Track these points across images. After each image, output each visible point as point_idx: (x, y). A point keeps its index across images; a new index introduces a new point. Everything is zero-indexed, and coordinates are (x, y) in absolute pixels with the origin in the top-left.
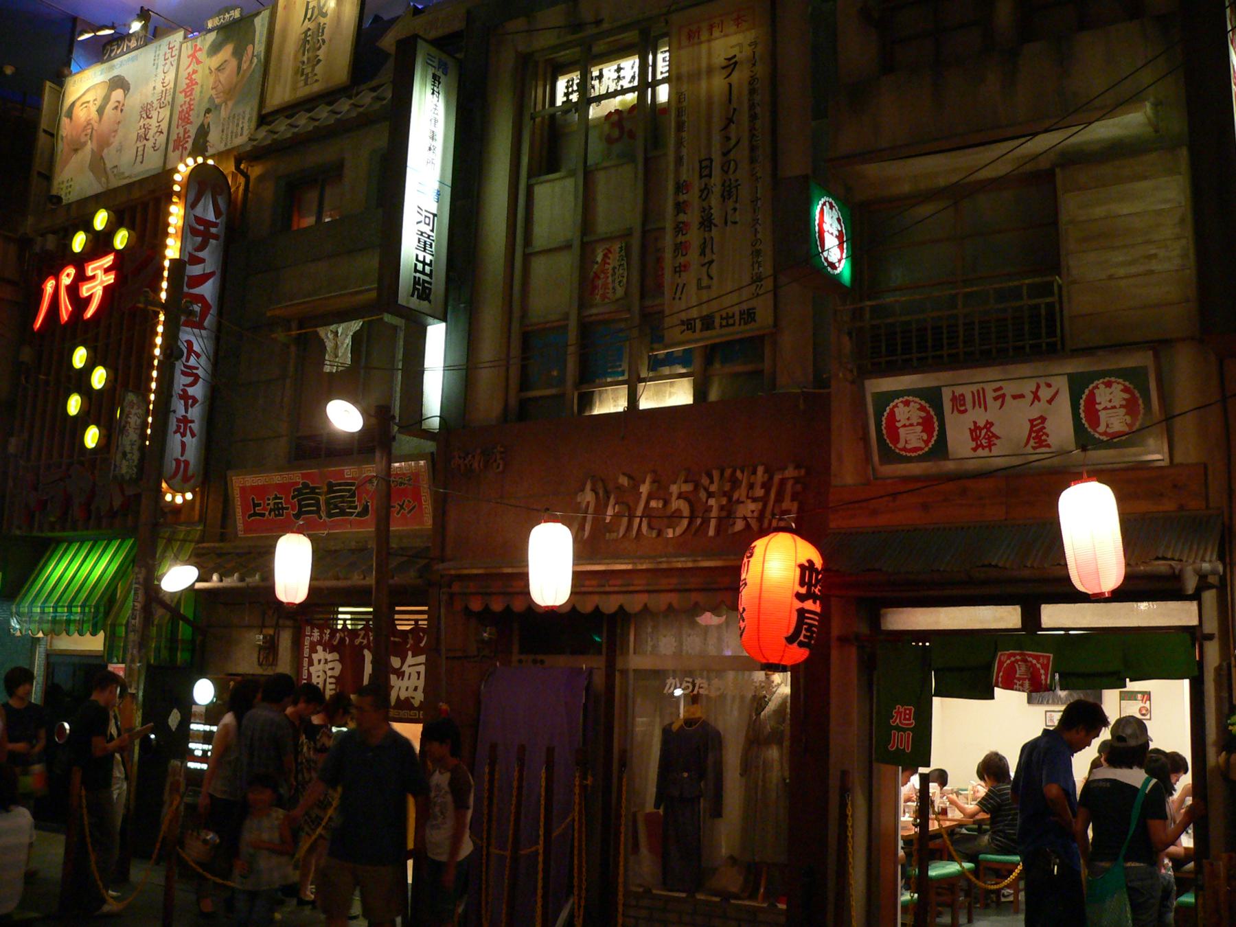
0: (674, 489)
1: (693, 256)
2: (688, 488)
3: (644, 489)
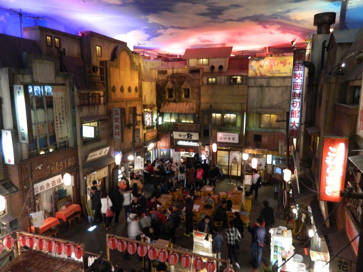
0: (61, 163)
1: (59, 128)
2: (62, 162)
3: (57, 164)
